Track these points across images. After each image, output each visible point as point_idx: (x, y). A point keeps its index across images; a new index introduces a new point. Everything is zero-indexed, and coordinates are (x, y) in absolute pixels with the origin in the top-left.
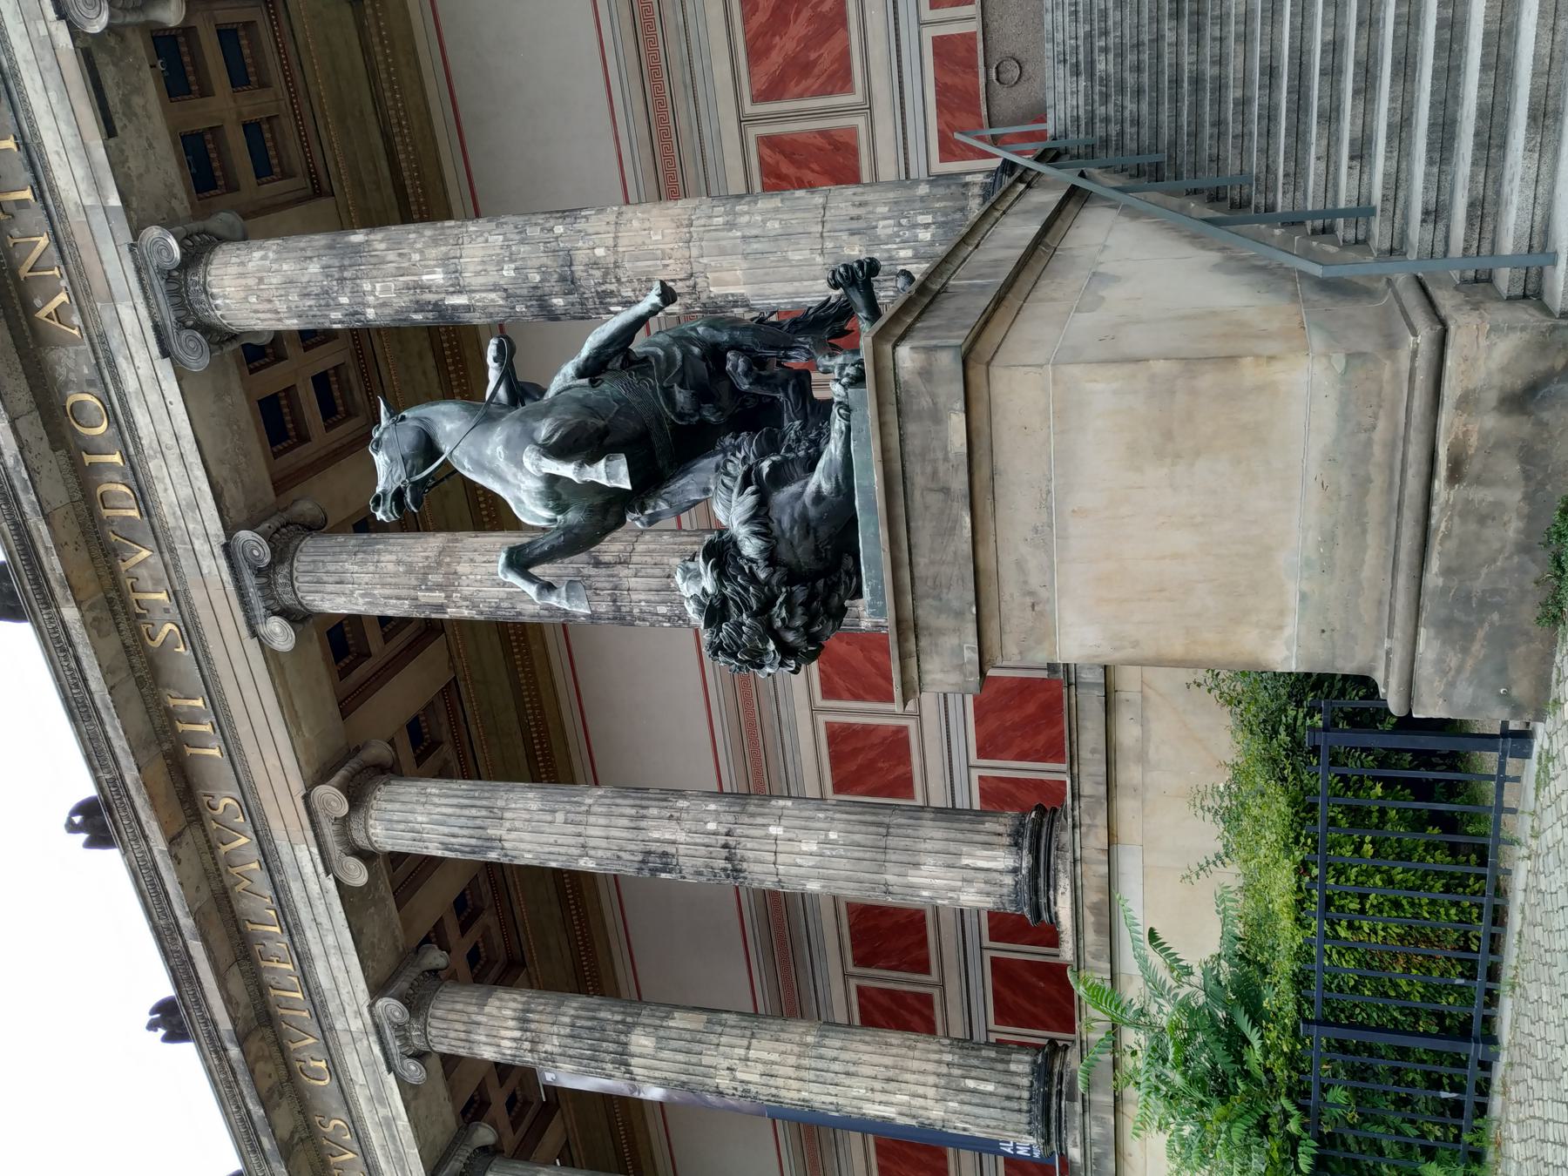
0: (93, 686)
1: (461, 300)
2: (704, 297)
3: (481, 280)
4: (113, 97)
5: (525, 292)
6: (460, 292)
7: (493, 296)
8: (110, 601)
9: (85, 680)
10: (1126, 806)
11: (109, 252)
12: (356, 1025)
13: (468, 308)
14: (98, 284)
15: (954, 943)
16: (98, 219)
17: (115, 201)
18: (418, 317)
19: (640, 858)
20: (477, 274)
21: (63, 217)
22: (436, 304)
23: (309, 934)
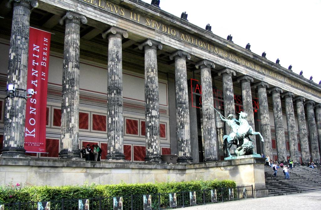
0: (149, 10)
1: (184, 93)
2: (185, 124)
4: (197, 58)
5: (185, 102)
6: (185, 93)
8: (153, 17)
9: (150, 9)
10: (137, 171)
11: (188, 49)
12: (79, 9)
13: (183, 93)
14: (185, 45)
15: (51, 131)
16: (190, 50)
17: (192, 54)
18: (182, 86)
19: (119, 88)
21: (191, 46)
22: (184, 89)
23: (99, 12)
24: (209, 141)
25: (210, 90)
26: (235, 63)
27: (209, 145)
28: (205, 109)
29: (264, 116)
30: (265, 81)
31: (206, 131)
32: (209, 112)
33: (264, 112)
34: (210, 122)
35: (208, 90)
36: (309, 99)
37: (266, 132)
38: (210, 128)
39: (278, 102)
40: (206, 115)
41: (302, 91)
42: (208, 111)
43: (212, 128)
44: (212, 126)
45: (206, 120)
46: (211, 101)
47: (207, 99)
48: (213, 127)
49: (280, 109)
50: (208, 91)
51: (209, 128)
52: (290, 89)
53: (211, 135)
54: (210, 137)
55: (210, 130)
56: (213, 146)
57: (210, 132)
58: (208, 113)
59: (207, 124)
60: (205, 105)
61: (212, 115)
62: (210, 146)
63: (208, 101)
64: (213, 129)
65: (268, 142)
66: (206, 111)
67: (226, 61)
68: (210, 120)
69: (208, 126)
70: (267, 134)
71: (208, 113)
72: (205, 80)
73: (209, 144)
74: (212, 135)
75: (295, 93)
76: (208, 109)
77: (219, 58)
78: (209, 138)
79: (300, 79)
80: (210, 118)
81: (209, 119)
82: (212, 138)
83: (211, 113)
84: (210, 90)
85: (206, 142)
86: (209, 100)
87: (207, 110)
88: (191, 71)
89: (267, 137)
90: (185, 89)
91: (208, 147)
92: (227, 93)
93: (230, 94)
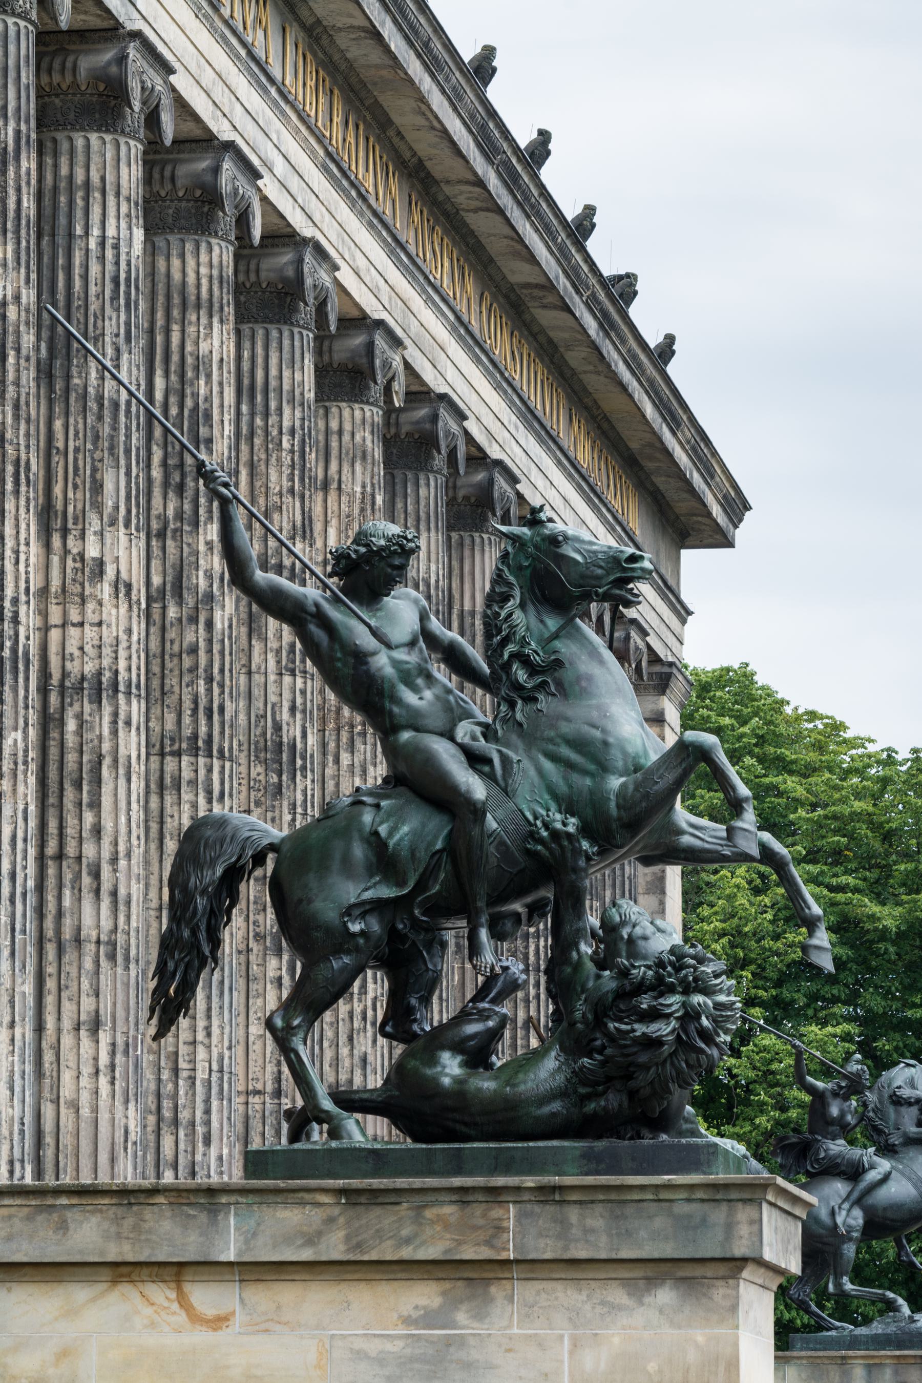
29: (92, 551)
30: (161, 48)
33: (98, 487)
36: (429, 376)
37: (95, 805)
39: (201, 365)
41: (395, 246)
65: (112, 957)
70: (108, 824)
75: (345, 276)
89: (96, 875)
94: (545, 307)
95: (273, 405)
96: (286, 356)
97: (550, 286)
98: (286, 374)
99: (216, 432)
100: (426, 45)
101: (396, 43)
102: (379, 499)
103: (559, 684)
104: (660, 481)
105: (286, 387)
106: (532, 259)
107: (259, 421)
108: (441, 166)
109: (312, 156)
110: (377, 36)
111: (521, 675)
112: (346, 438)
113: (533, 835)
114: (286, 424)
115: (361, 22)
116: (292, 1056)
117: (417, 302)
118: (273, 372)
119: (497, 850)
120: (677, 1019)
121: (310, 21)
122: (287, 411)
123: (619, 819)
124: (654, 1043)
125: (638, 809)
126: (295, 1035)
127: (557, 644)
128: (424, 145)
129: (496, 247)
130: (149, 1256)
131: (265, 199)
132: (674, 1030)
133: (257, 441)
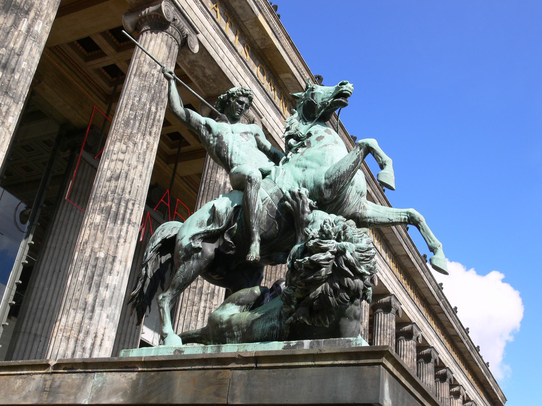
3: (28, 48)
5: (13, 63)
7: (18, 46)
13: (15, 25)
20: (31, 50)
22: (27, 13)
24: (79, 316)
25: (153, 109)
26: (267, 100)
27: (74, 333)
28: (109, 174)
31: (83, 267)
32: (123, 190)
34: (112, 231)
35: (145, 105)
38: (106, 258)
40: (105, 198)
42: (121, 183)
43: (114, 258)
44: (115, 252)
45: (98, 218)
46: (145, 153)
47: (130, 137)
48: (119, 257)
49: (364, 330)
50: (143, 109)
51: (102, 255)
52: (395, 289)
53: (97, 291)
54: (90, 299)
55: (100, 264)
56: (93, 345)
57: (101, 275)
58: (114, 192)
59: (96, 235)
60: (114, 157)
61: (130, 206)
62: (77, 340)
63: (131, 145)
64: (117, 267)
66: (110, 180)
67: (240, 69)
68: (115, 222)
69: (96, 246)
71: (114, 192)
72: (145, 68)
73: (76, 328)
74: (105, 294)
75: (402, 306)
76: (123, 175)
77: (220, 41)
78: (86, 303)
79: (422, 274)
80: (117, 214)
81: (114, 216)
82: (102, 306)
83: (127, 196)
84: (153, 109)
85: (64, 320)
86: (135, 144)
87: (118, 178)
88: (106, 103)
90: (32, 14)
91: (64, 344)
92: (218, 176)
93: (225, 183)
94: (458, 342)
95: (385, 329)
96: (388, 319)
97: (457, 335)
98: (388, 322)
99: (363, 320)
100: (421, 264)
101: (413, 260)
102: (415, 360)
103: (309, 143)
104: (488, 390)
105: (388, 325)
106: (454, 328)
107: (382, 332)
108: (430, 300)
109: (395, 280)
110: (408, 256)
111: (292, 141)
112: (408, 347)
113: (285, 198)
114: (388, 333)
115: (405, 253)
116: (161, 310)
117: (426, 326)
118: (385, 322)
119: (267, 207)
120: (332, 253)
121: (394, 252)
122: (388, 330)
123: (326, 184)
124: (317, 266)
125: (334, 177)
126: (164, 300)
127: (310, 130)
128: (426, 294)
129: (445, 324)
130: (52, 401)
131: (378, 277)
132: (328, 259)
133: (382, 336)
